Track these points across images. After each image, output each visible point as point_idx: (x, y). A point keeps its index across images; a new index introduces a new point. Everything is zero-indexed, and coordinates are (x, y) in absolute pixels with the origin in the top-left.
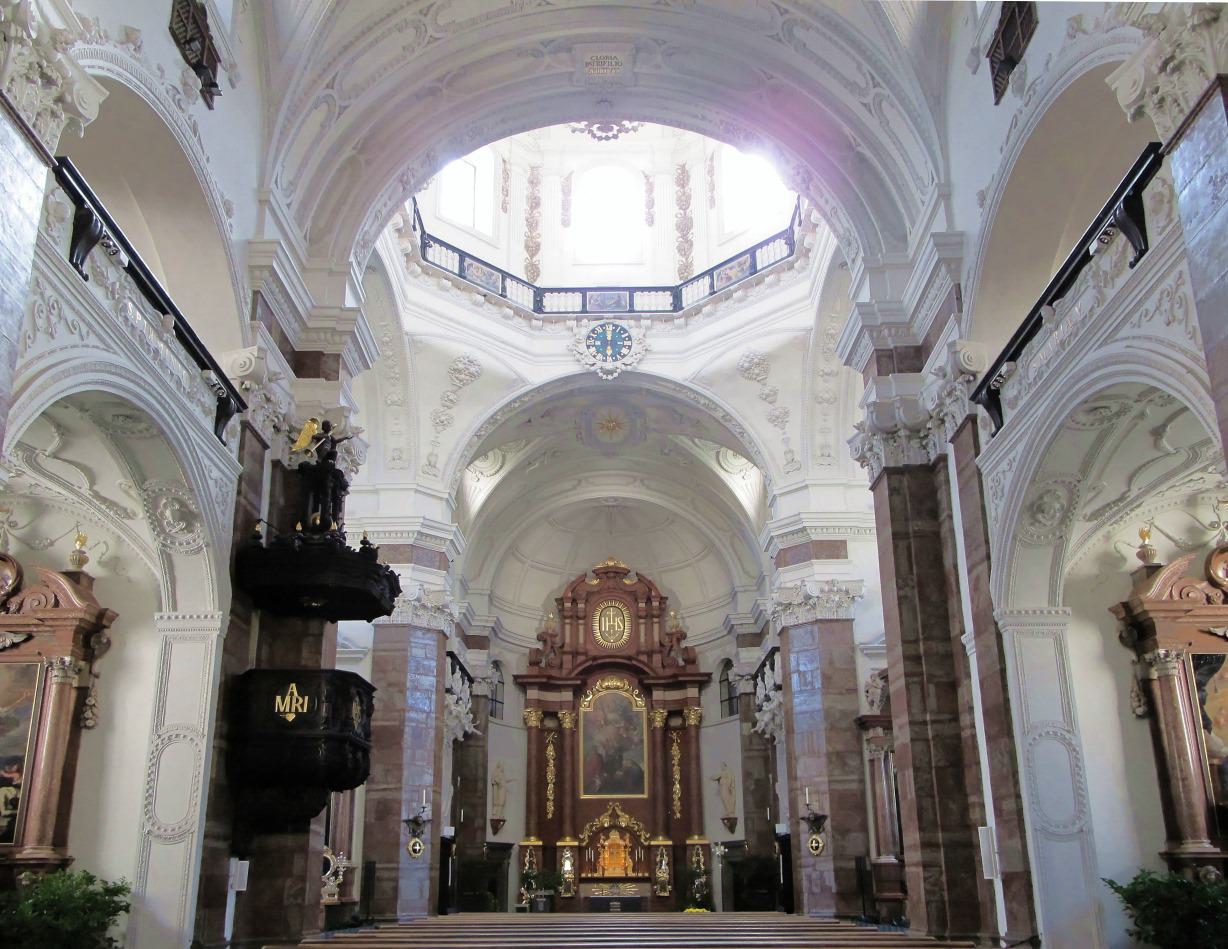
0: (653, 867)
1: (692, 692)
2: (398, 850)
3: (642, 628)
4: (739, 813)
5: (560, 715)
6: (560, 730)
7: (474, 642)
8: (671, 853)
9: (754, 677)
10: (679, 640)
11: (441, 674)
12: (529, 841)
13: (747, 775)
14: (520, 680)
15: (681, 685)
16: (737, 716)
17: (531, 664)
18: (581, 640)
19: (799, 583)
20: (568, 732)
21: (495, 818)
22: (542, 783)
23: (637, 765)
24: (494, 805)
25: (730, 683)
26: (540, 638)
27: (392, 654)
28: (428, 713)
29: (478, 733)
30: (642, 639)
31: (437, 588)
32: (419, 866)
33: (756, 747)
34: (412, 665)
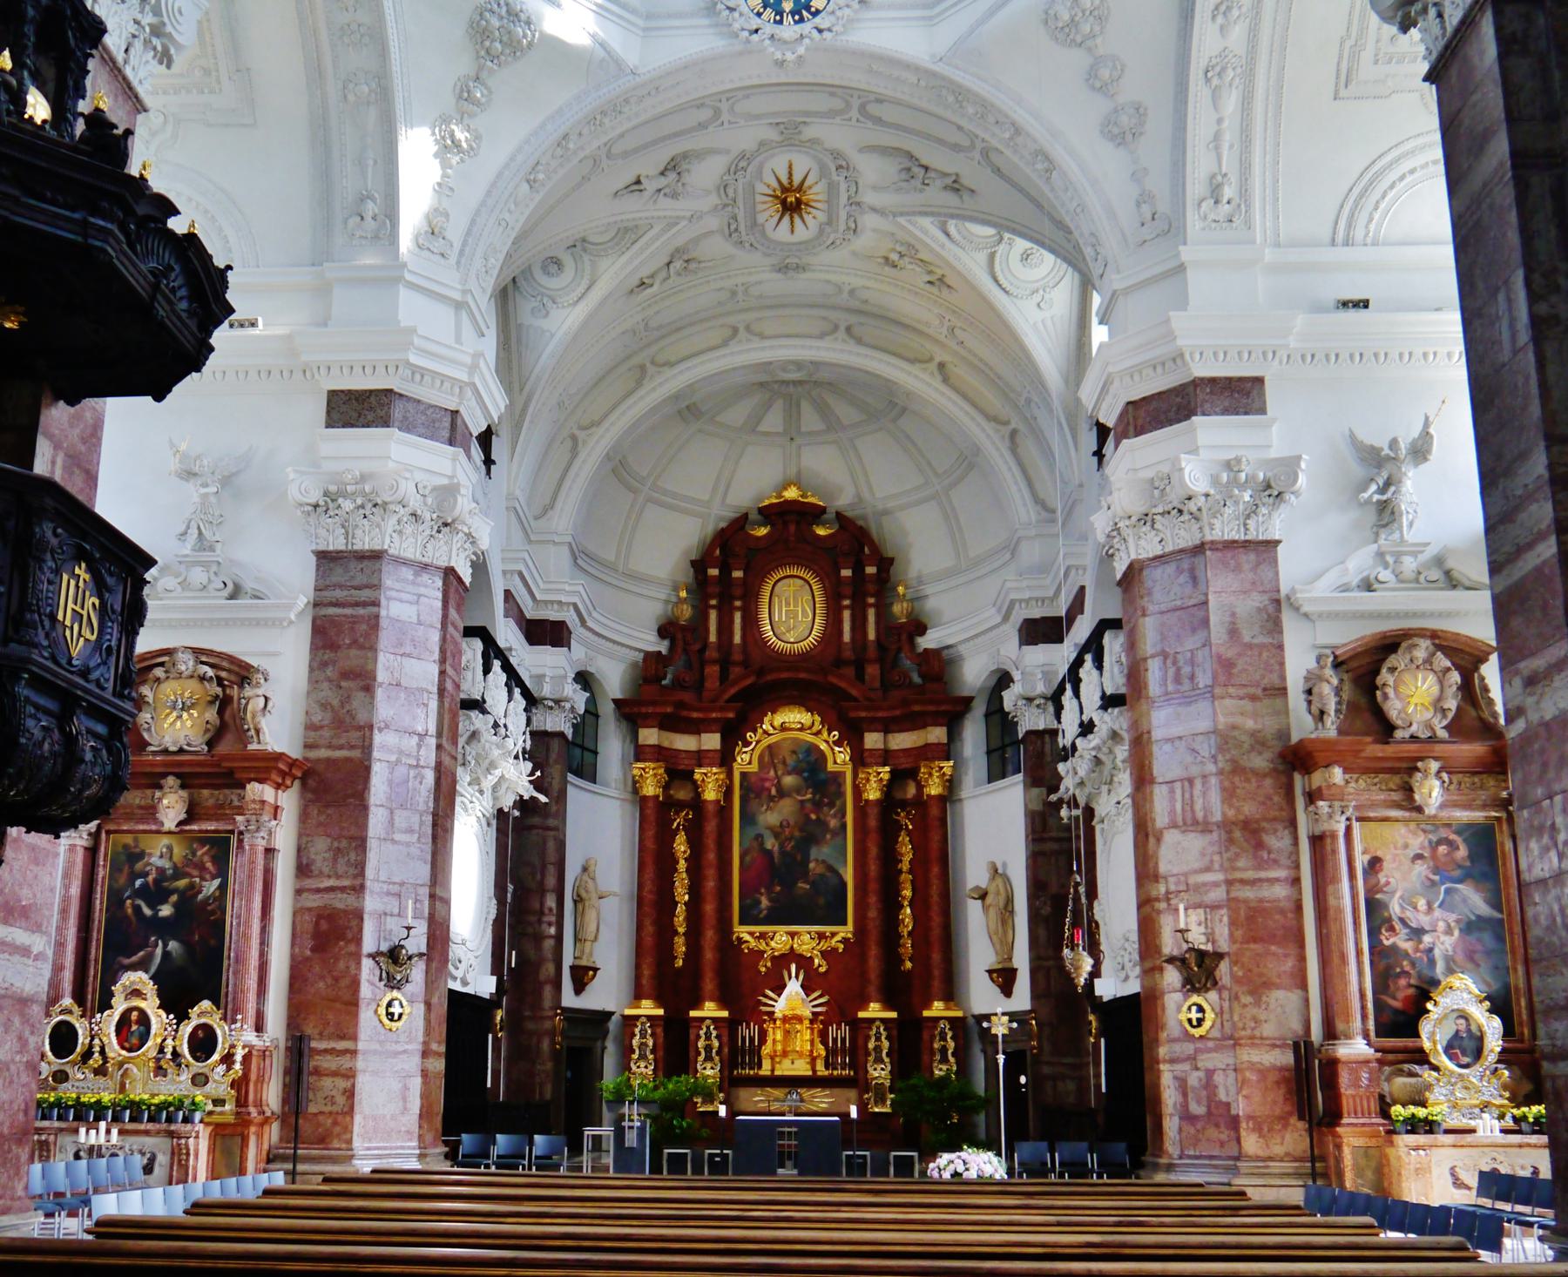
1: (937, 734)
2: (356, 1015)
3: (847, 614)
4: (1021, 960)
5: (697, 777)
6: (697, 803)
11: (448, 656)
13: (1036, 886)
14: (627, 710)
16: (1020, 777)
18: (737, 639)
19: (1166, 469)
20: (711, 808)
21: (578, 962)
22: (665, 903)
24: (577, 939)
26: (664, 631)
27: (348, 611)
28: (422, 736)
29: (543, 799)
30: (847, 637)
31: (445, 481)
32: (399, 1048)
33: (1054, 834)
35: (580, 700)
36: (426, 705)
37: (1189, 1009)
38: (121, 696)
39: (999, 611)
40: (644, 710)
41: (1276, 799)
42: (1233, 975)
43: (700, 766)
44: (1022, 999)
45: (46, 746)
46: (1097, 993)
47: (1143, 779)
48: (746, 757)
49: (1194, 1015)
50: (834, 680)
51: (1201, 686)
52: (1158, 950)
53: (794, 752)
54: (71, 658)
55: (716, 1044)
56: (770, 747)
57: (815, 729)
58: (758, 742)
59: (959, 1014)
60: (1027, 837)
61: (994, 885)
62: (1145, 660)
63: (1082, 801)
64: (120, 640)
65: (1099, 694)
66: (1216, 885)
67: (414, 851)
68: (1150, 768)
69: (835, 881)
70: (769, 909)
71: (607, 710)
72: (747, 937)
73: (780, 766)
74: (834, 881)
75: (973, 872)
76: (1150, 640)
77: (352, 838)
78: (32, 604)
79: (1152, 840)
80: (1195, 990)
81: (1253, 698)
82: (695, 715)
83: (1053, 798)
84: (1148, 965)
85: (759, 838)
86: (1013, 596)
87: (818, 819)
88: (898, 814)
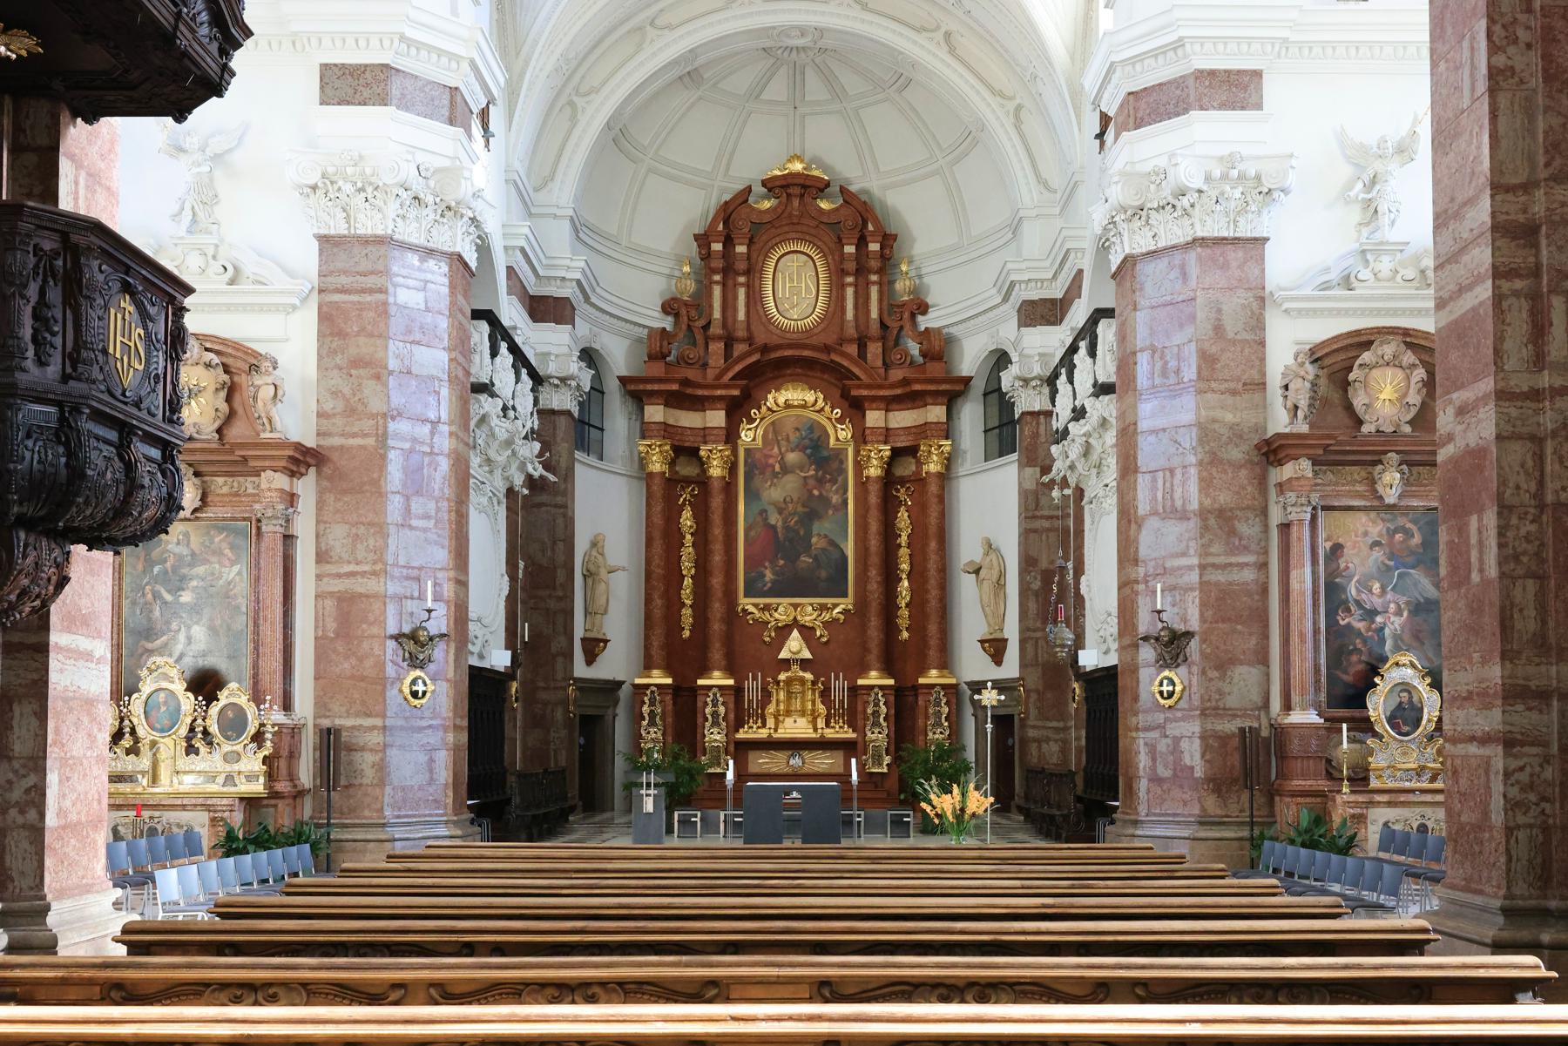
0: (860, 723)
1: (936, 413)
3: (850, 291)
4: (1012, 632)
5: (702, 453)
6: (703, 481)
7: (544, 309)
8: (892, 698)
9: (1051, 381)
10: (913, 316)
11: (461, 347)
12: (649, 677)
13: (1028, 562)
14: (633, 387)
15: (911, 399)
16: (1015, 456)
17: (652, 357)
18: (741, 315)
20: (716, 486)
21: (589, 635)
23: (837, 546)
25: (1002, 395)
28: (435, 424)
29: (552, 478)
30: (850, 314)
33: (1046, 513)
34: (396, 325)
35: (586, 378)
36: (438, 393)
37: (1161, 684)
38: (171, 421)
39: (999, 292)
40: (649, 387)
41: (1249, 489)
42: (1202, 652)
43: (705, 443)
44: (1010, 668)
45: (109, 475)
46: (1081, 663)
47: (1128, 468)
48: (751, 433)
49: (1165, 688)
50: (837, 359)
51: (1185, 380)
52: (1135, 627)
53: (797, 429)
54: (124, 391)
55: (722, 709)
56: (773, 423)
57: (817, 408)
58: (762, 419)
59: (953, 681)
60: (1020, 515)
61: (988, 559)
62: (1134, 353)
63: (1072, 481)
64: (166, 368)
65: (1092, 382)
66: (1190, 568)
67: (432, 536)
68: (1135, 458)
69: (835, 555)
70: (774, 582)
71: (612, 386)
72: (751, 609)
73: (783, 443)
74: (835, 555)
75: (967, 549)
76: (1141, 336)
77: (371, 524)
78: (86, 342)
79: (1133, 526)
80: (1167, 666)
81: (1234, 393)
82: (700, 392)
83: (1046, 479)
84: (1127, 641)
85: (763, 512)
86: (1013, 277)
87: (821, 494)
88: (898, 491)
